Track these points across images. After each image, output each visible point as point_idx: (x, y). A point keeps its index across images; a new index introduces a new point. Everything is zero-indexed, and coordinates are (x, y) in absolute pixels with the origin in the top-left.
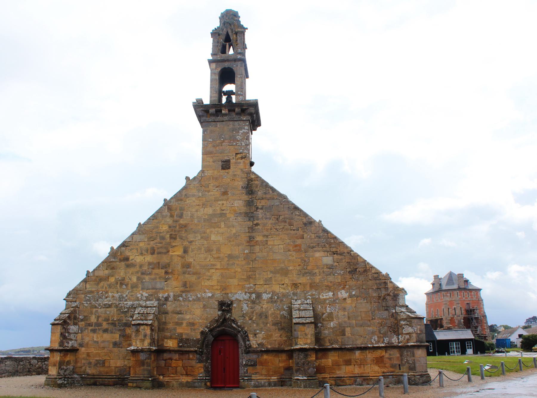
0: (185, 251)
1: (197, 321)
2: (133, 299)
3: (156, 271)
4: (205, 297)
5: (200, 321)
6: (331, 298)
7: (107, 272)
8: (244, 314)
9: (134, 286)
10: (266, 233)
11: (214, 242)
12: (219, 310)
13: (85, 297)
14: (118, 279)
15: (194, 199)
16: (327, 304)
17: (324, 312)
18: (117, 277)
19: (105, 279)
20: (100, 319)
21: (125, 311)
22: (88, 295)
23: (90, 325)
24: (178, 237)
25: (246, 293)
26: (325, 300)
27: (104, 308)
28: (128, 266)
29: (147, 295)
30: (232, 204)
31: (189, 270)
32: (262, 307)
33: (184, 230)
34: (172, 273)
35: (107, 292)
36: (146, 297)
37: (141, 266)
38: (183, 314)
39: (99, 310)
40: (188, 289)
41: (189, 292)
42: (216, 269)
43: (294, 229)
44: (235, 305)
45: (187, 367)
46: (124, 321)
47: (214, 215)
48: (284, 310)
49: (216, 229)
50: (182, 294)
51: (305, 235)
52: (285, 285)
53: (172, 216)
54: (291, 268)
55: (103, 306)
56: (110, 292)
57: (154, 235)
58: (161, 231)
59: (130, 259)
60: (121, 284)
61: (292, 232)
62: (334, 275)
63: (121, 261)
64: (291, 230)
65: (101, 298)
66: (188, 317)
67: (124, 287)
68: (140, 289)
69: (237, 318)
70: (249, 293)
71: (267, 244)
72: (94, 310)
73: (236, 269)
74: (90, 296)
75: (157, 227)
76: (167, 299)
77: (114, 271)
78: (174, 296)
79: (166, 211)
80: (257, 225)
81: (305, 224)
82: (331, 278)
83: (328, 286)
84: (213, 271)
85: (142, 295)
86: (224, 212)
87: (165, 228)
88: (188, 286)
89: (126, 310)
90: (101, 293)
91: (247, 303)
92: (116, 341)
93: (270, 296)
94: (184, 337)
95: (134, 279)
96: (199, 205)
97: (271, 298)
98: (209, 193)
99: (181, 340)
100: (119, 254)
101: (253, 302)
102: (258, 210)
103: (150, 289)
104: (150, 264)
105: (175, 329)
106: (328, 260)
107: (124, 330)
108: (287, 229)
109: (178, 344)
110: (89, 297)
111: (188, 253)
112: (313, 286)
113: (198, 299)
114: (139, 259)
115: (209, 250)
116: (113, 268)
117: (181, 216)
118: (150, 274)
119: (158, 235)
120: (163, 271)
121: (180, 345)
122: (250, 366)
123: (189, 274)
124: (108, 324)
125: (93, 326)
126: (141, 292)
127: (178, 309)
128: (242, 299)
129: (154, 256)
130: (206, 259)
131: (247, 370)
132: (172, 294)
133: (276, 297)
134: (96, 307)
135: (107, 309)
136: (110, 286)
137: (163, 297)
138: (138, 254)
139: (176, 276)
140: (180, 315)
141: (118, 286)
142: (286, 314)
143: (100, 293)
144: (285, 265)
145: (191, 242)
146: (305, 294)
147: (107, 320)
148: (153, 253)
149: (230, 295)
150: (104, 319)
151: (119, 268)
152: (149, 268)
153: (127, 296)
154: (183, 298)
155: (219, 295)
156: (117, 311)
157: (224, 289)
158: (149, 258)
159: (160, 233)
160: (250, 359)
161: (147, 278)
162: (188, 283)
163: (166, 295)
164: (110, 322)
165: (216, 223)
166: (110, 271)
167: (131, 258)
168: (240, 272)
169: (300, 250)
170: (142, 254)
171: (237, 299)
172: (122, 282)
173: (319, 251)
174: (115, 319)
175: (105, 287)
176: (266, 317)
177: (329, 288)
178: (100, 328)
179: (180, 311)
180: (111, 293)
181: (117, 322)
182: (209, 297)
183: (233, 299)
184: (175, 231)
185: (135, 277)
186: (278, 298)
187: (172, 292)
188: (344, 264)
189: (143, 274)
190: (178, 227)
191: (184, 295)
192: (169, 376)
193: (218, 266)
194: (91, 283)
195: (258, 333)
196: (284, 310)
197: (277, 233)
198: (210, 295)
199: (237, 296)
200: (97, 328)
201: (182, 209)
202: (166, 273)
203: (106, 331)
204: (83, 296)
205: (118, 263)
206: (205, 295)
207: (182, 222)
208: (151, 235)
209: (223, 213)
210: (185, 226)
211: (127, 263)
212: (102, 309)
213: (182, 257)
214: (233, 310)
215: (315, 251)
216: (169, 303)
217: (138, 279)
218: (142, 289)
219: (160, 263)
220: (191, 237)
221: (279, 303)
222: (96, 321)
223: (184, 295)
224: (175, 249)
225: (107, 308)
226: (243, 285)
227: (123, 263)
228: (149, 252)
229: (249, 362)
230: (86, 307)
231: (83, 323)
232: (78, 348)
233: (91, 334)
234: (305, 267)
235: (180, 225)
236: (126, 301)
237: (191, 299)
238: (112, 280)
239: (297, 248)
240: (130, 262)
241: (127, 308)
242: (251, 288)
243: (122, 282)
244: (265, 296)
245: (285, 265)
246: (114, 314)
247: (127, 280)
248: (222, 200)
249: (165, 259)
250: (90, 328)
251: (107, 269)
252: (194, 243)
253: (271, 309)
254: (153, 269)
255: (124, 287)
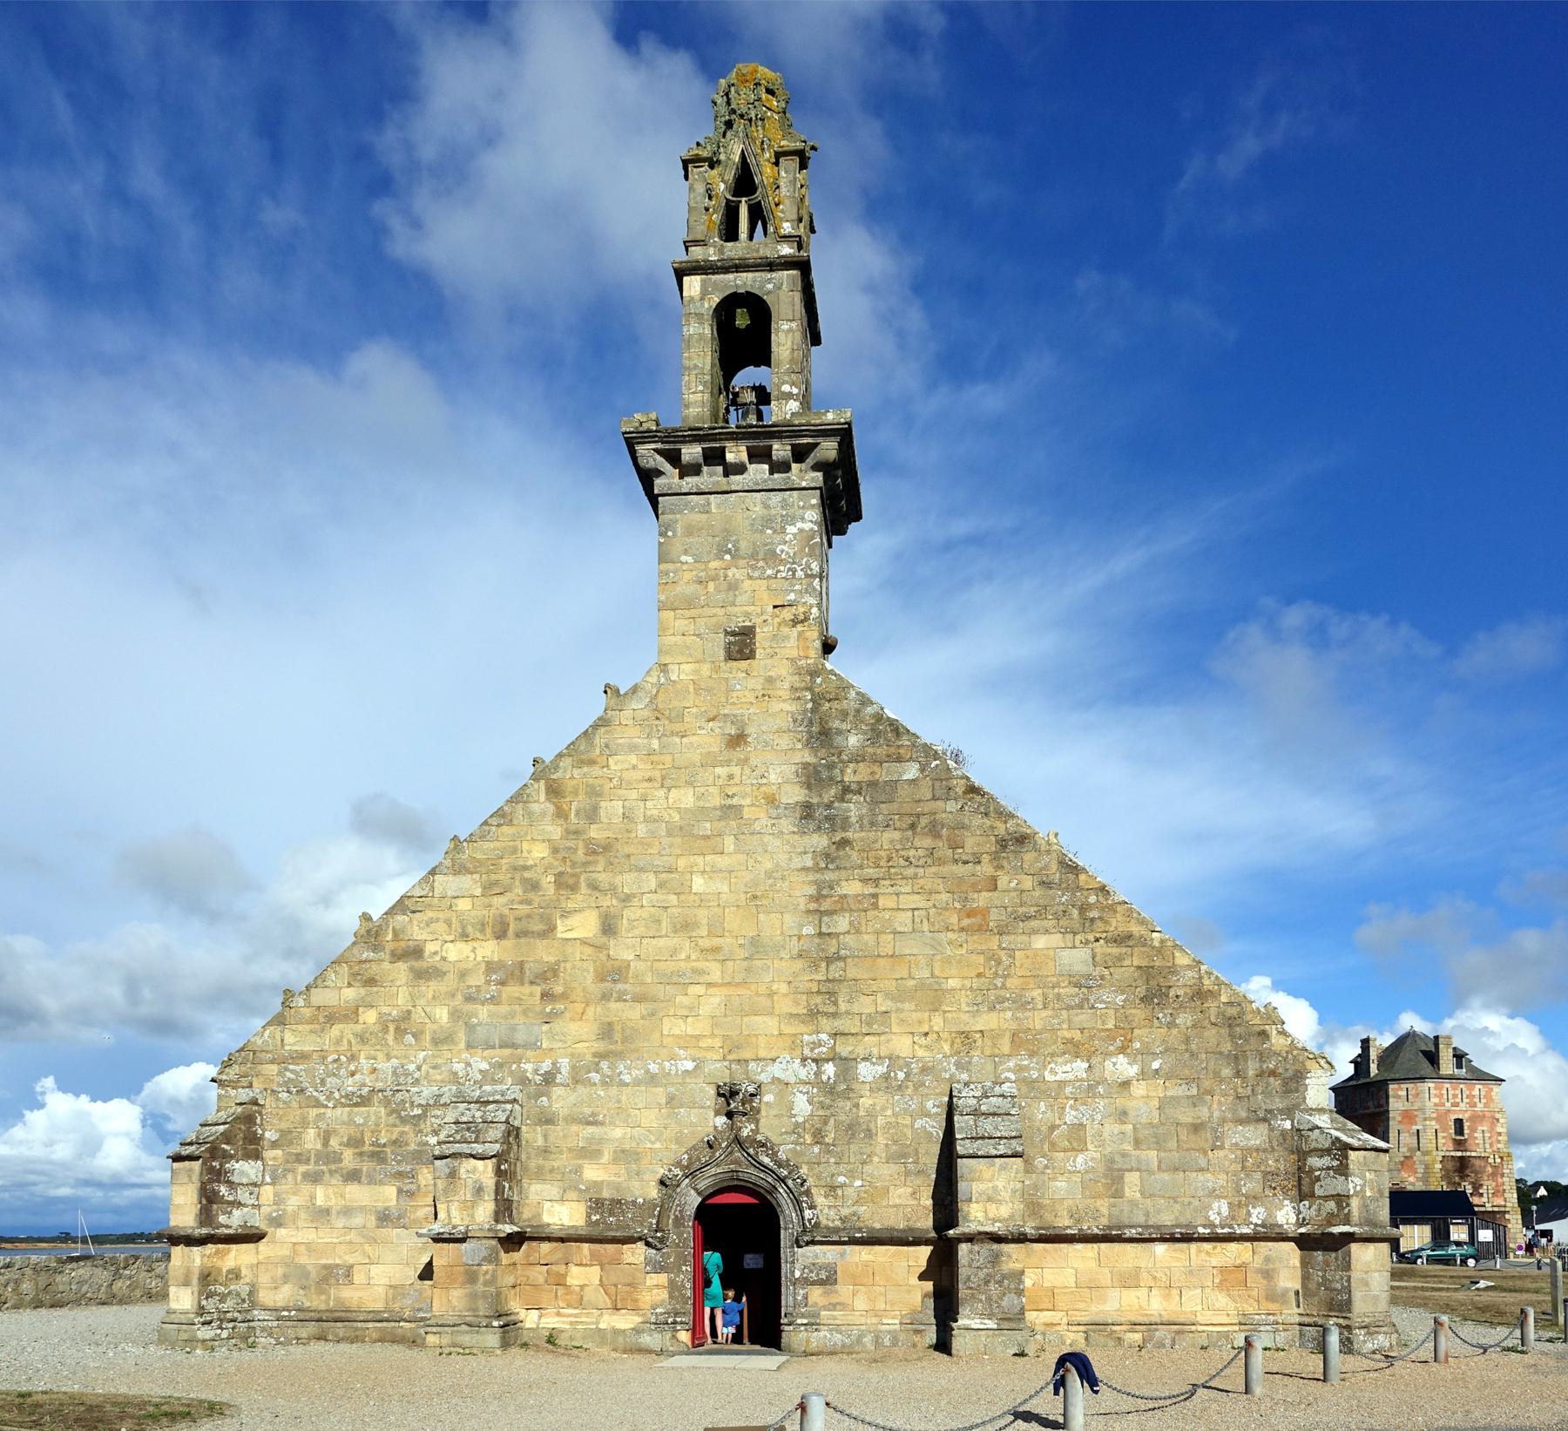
0: (608, 927)
1: (649, 1146)
2: (439, 1077)
3: (512, 990)
4: (673, 1072)
5: (658, 1145)
6: (1082, 1080)
7: (350, 994)
8: (797, 1125)
9: (442, 1040)
10: (871, 872)
11: (702, 900)
12: (717, 1113)
13: (280, 1074)
14: (390, 1014)
15: (633, 759)
16: (1067, 1098)
17: (1058, 1122)
18: (386, 1010)
19: (346, 1016)
20: (334, 1142)
21: (414, 1116)
22: (291, 1067)
23: (300, 1158)
24: (583, 885)
25: (804, 1060)
26: (1062, 1084)
27: (344, 1105)
28: (421, 975)
29: (485, 1066)
30: (763, 776)
31: (620, 986)
32: (857, 1106)
33: (602, 860)
34: (564, 996)
35: (353, 1058)
36: (481, 1071)
37: (463, 975)
38: (602, 1124)
39: (329, 1112)
40: (619, 1047)
41: (620, 1055)
42: (710, 985)
43: (965, 858)
44: (768, 1098)
45: (616, 1286)
46: (413, 1147)
47: (701, 812)
48: (928, 1115)
49: (708, 858)
50: (597, 1064)
51: (1003, 881)
52: (932, 1037)
53: (561, 814)
54: (952, 983)
55: (343, 1100)
56: (362, 1056)
57: (503, 877)
58: (531, 862)
59: (427, 954)
60: (400, 1033)
61: (960, 870)
62: (1093, 1007)
63: (397, 957)
64: (956, 861)
65: (334, 1075)
66: (618, 1133)
67: (409, 1038)
68: (462, 1045)
69: (775, 1139)
70: (814, 1060)
71: (875, 906)
72: (313, 1112)
73: (775, 987)
74: (297, 1068)
75: (514, 851)
76: (549, 1079)
77: (375, 989)
78: (573, 1067)
79: (542, 797)
80: (844, 843)
81: (1002, 844)
82: (1082, 1018)
83: (1070, 1041)
84: (700, 990)
85: (468, 1064)
86: (735, 801)
87: (537, 852)
88: (618, 1036)
89: (417, 1111)
90: (335, 1061)
91: (807, 1093)
92: (387, 1209)
93: (882, 1069)
94: (606, 1194)
95: (442, 1014)
96: (650, 780)
97: (886, 1077)
98: (685, 740)
99: (597, 1204)
100: (390, 937)
101: (830, 1090)
102: (848, 796)
103: (493, 1047)
104: (490, 967)
105: (578, 1170)
106: (1076, 958)
107: (412, 1175)
108: (941, 862)
109: (589, 1216)
110: (292, 1071)
111: (615, 933)
112: (1019, 1040)
113: (652, 1080)
114: (456, 952)
115: (685, 926)
116: (371, 982)
117: (592, 815)
118: (494, 1000)
119: (518, 877)
120: (538, 990)
121: (594, 1218)
122: (813, 1283)
123: (619, 1000)
124: (361, 1154)
125: (312, 1161)
126: (465, 1055)
127: (588, 1111)
128: (792, 1080)
129: (504, 943)
130: (674, 952)
131: (806, 1297)
132: (565, 1064)
133: (901, 1075)
134: (318, 1104)
135: (356, 1109)
136: (362, 1039)
137: (536, 1071)
138: (452, 938)
139: (579, 1007)
140: (591, 1129)
141: (390, 1037)
142: (933, 1127)
143: (330, 1059)
144: (933, 975)
145: (627, 899)
146: (996, 1066)
147: (355, 1142)
148: (501, 934)
149: (752, 1065)
150: (345, 1140)
151: (392, 981)
152: (488, 982)
153: (419, 1068)
154: (603, 1075)
155: (719, 1071)
156: (388, 1115)
157: (732, 1046)
158: (489, 949)
159: (526, 868)
160: (814, 1265)
161: (483, 1013)
162: (617, 1028)
163: (546, 1066)
164: (367, 1148)
165: (708, 837)
166: (363, 991)
167: (430, 948)
168: (785, 995)
169: (981, 929)
170: (464, 936)
171: (775, 1080)
172: (402, 1025)
173: (1047, 932)
174: (383, 1141)
175: (345, 1041)
176: (870, 1134)
177: (1074, 1049)
178: (333, 1167)
179: (593, 1114)
180: (368, 1058)
181: (388, 1150)
182: (687, 1071)
183: (763, 1078)
184: (574, 865)
185: (445, 1010)
186: (907, 1075)
187: (566, 1056)
188: (1123, 973)
189: (469, 999)
190: (580, 852)
191: (604, 1065)
192: (558, 1314)
193: (716, 976)
194: (300, 1027)
195: (842, 1186)
196: (928, 1115)
197: (910, 871)
198: (690, 1065)
199: (776, 1070)
200: (324, 1167)
201: (594, 793)
202: (546, 996)
203: (353, 1176)
204: (274, 1068)
205: (386, 965)
206: (673, 1068)
207: (595, 832)
208: (493, 877)
209: (731, 807)
210: (607, 847)
211: (417, 964)
212: (339, 1111)
213: (599, 948)
214: (763, 1113)
215: (1035, 932)
216: (557, 1091)
217: (455, 1015)
218: (469, 1046)
219: (527, 966)
220: (627, 882)
221: (910, 1091)
222: (319, 1147)
223: (604, 1065)
224: (574, 920)
225: (356, 1105)
226: (795, 1035)
227: (402, 966)
228: (489, 930)
229: (812, 1271)
230: (285, 1103)
231: (279, 1153)
232: (263, 1226)
233: (306, 1188)
234: (999, 982)
235: (589, 842)
236: (417, 1082)
237: (627, 1078)
238: (370, 1017)
239: (975, 919)
240: (429, 961)
241: (420, 1105)
242: (820, 1045)
243: (402, 1025)
244: (866, 1071)
245: (933, 975)
246: (377, 1125)
247: (418, 1016)
248: (728, 763)
249: (543, 953)
250: (302, 1169)
251: (350, 985)
252: (635, 902)
253: (884, 1109)
254: (502, 983)
255: (409, 1038)
